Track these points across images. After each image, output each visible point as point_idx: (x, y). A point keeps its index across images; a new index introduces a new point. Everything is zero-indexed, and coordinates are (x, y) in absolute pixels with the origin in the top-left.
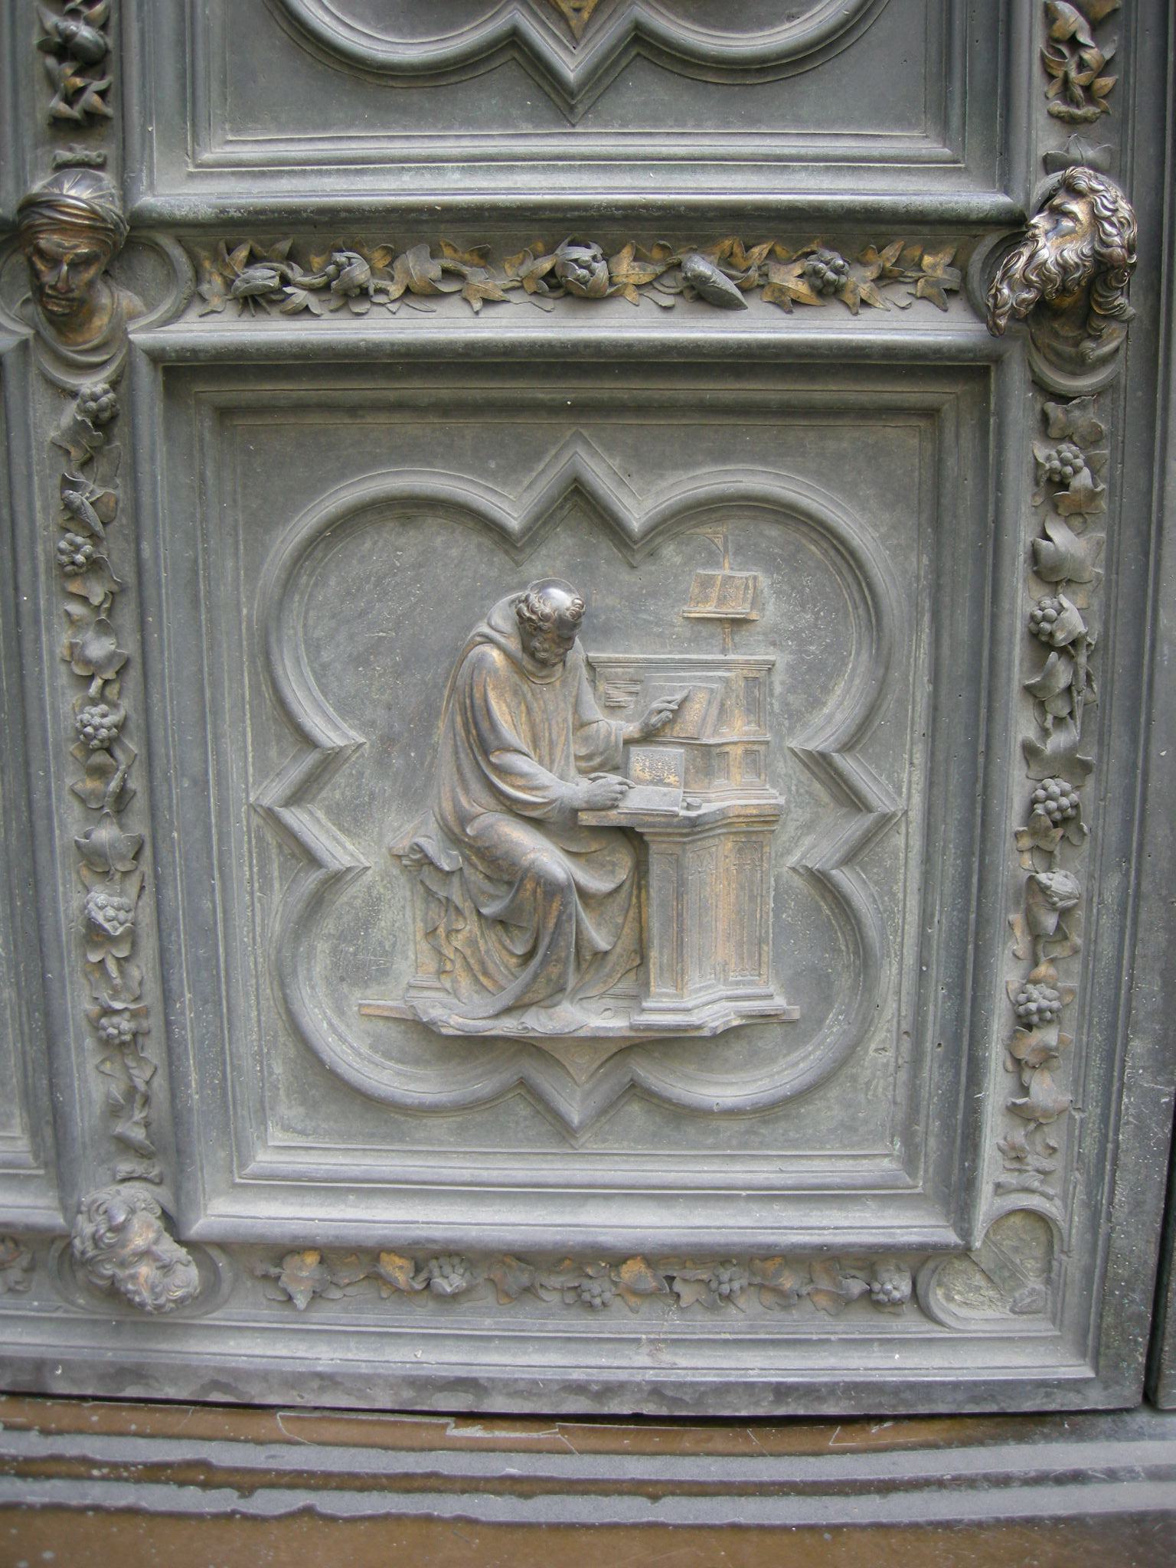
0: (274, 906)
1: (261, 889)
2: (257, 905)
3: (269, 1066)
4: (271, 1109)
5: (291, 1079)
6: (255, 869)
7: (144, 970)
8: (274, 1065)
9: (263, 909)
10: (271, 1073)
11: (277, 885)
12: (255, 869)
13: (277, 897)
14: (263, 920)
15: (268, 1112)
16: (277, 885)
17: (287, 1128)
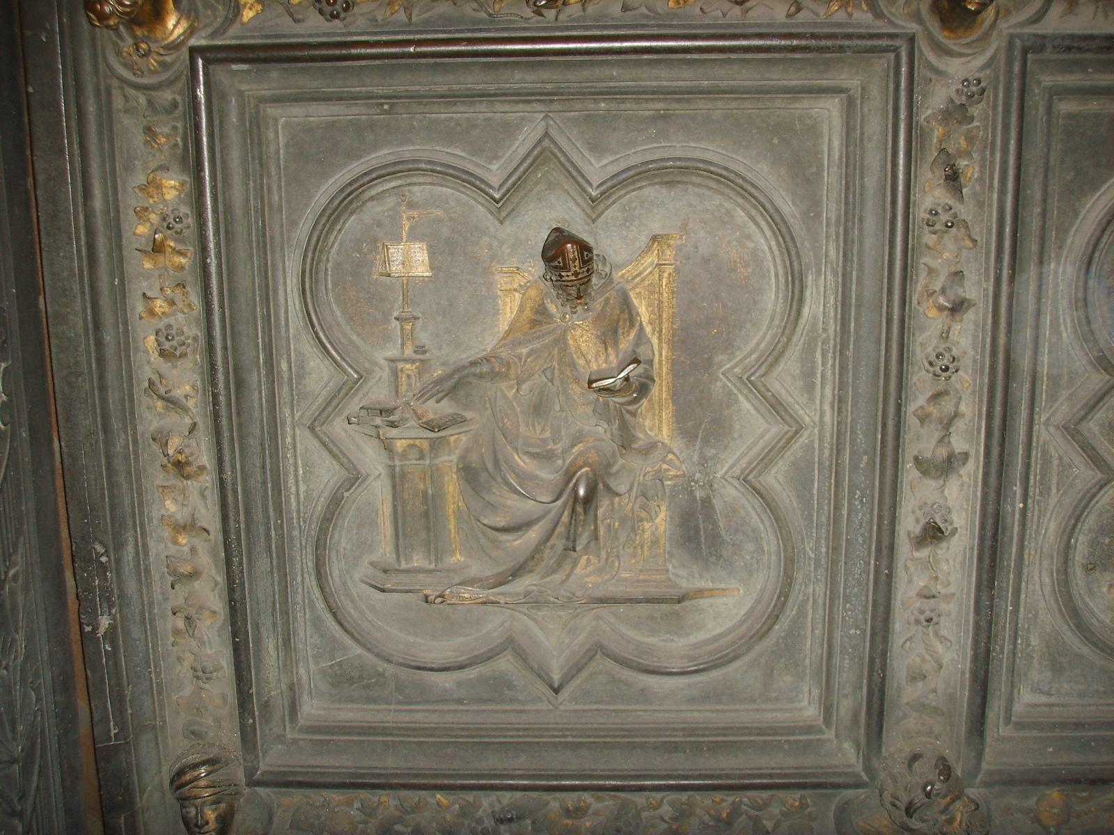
0: (1050, 508)
1: (1041, 493)
2: (1036, 507)
3: (1028, 639)
4: (1025, 675)
5: (1045, 649)
6: (1038, 477)
7: (951, 563)
8: (1032, 639)
9: (1040, 510)
10: (1028, 646)
11: (1054, 490)
12: (1038, 477)
13: (1053, 500)
14: (1039, 518)
15: (1023, 677)
16: (1054, 490)
17: (1037, 690)
